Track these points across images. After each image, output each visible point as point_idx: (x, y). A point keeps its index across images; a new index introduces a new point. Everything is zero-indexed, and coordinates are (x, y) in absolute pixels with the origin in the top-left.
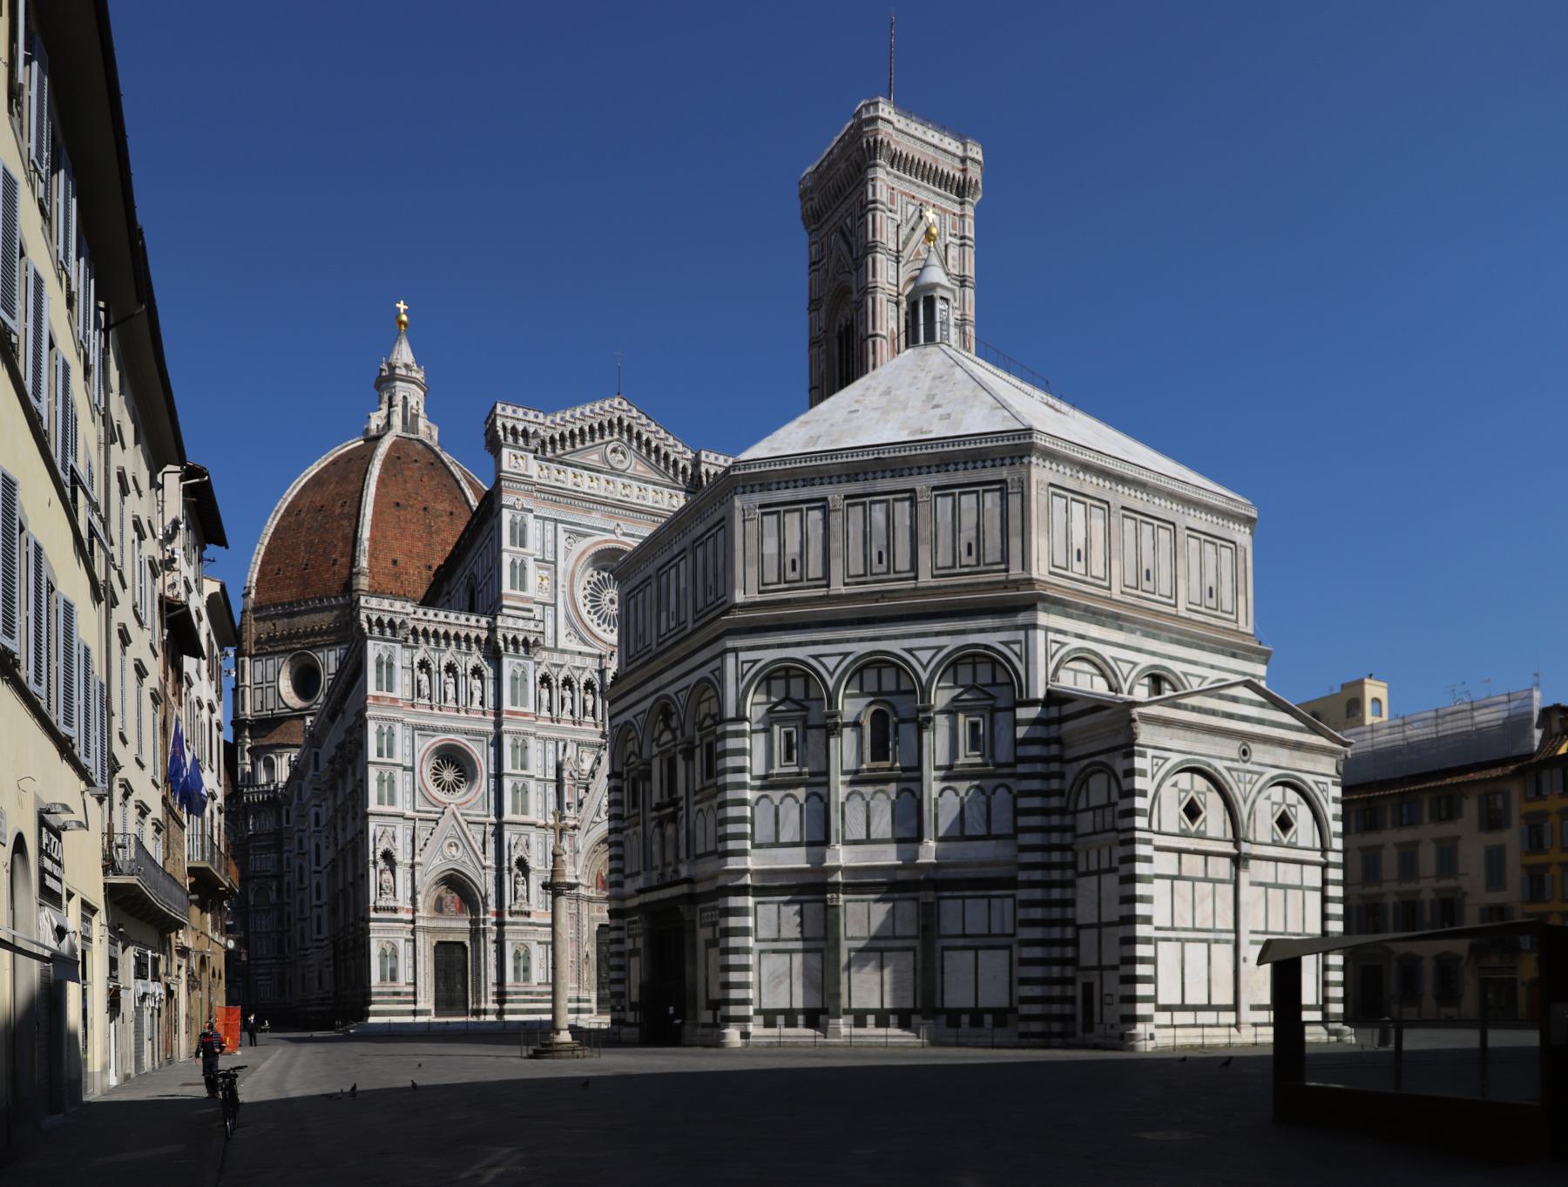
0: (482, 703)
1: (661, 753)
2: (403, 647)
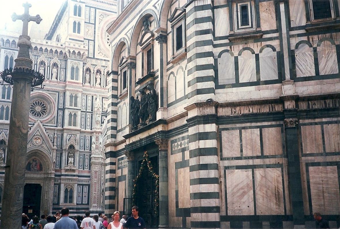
0: (57, 78)
1: (143, 49)
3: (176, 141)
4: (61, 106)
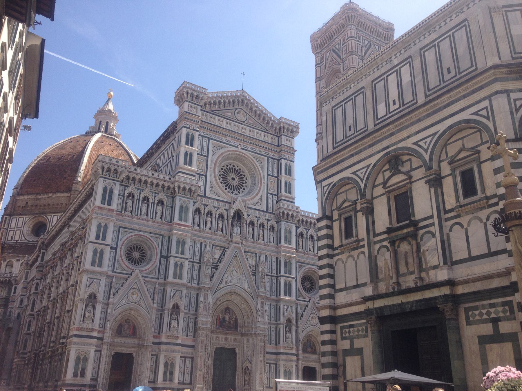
0: (161, 218)
2: (120, 185)
3: (476, 308)
4: (164, 253)
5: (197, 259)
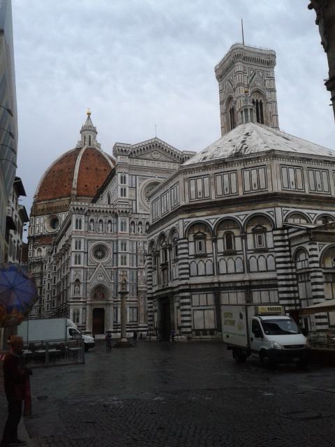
1: (163, 249)
4: (115, 251)
5: (135, 252)
